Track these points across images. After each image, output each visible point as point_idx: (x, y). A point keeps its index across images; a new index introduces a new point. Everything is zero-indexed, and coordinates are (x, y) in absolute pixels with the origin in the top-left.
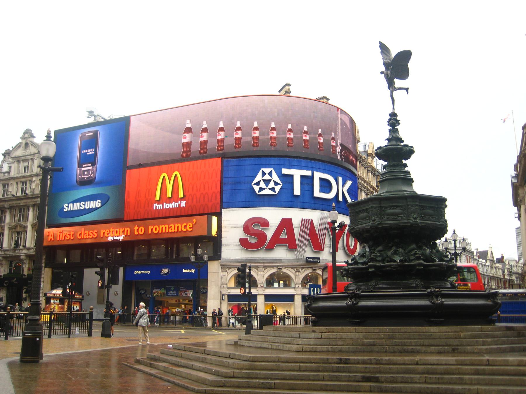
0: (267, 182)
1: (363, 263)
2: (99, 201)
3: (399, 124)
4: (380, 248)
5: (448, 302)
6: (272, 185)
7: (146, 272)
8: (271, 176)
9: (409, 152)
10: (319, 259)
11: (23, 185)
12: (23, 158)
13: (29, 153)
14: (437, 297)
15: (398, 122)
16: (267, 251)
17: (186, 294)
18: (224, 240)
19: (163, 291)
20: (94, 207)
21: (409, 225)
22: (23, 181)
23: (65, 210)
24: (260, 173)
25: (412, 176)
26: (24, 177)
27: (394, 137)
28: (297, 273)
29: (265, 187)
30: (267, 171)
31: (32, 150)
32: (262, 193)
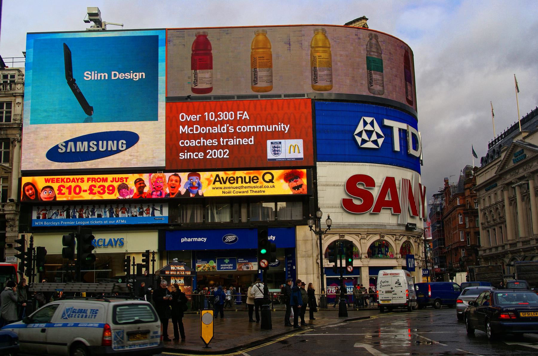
0: (369, 133)
2: (124, 142)
6: (374, 137)
7: (200, 240)
8: (373, 126)
10: (415, 225)
16: (371, 214)
17: (248, 268)
18: (321, 202)
19: (212, 264)
20: (115, 149)
23: (60, 151)
24: (362, 122)
28: (397, 242)
29: (368, 140)
30: (369, 120)
32: (365, 146)
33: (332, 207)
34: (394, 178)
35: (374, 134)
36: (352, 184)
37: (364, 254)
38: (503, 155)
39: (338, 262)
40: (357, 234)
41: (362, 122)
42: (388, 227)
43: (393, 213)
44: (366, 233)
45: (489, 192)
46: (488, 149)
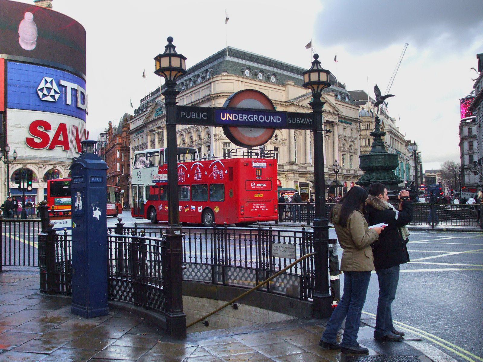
0: (49, 89)
6: (52, 93)
8: (52, 85)
16: (48, 150)
24: (43, 81)
29: (47, 94)
30: (49, 79)
32: (44, 99)
33: (18, 143)
34: (65, 124)
35: (53, 91)
36: (34, 127)
37: (41, 179)
38: (149, 109)
39: (22, 184)
40: (36, 164)
41: (44, 80)
42: (59, 160)
43: (63, 149)
44: (43, 164)
45: (139, 135)
46: (140, 104)
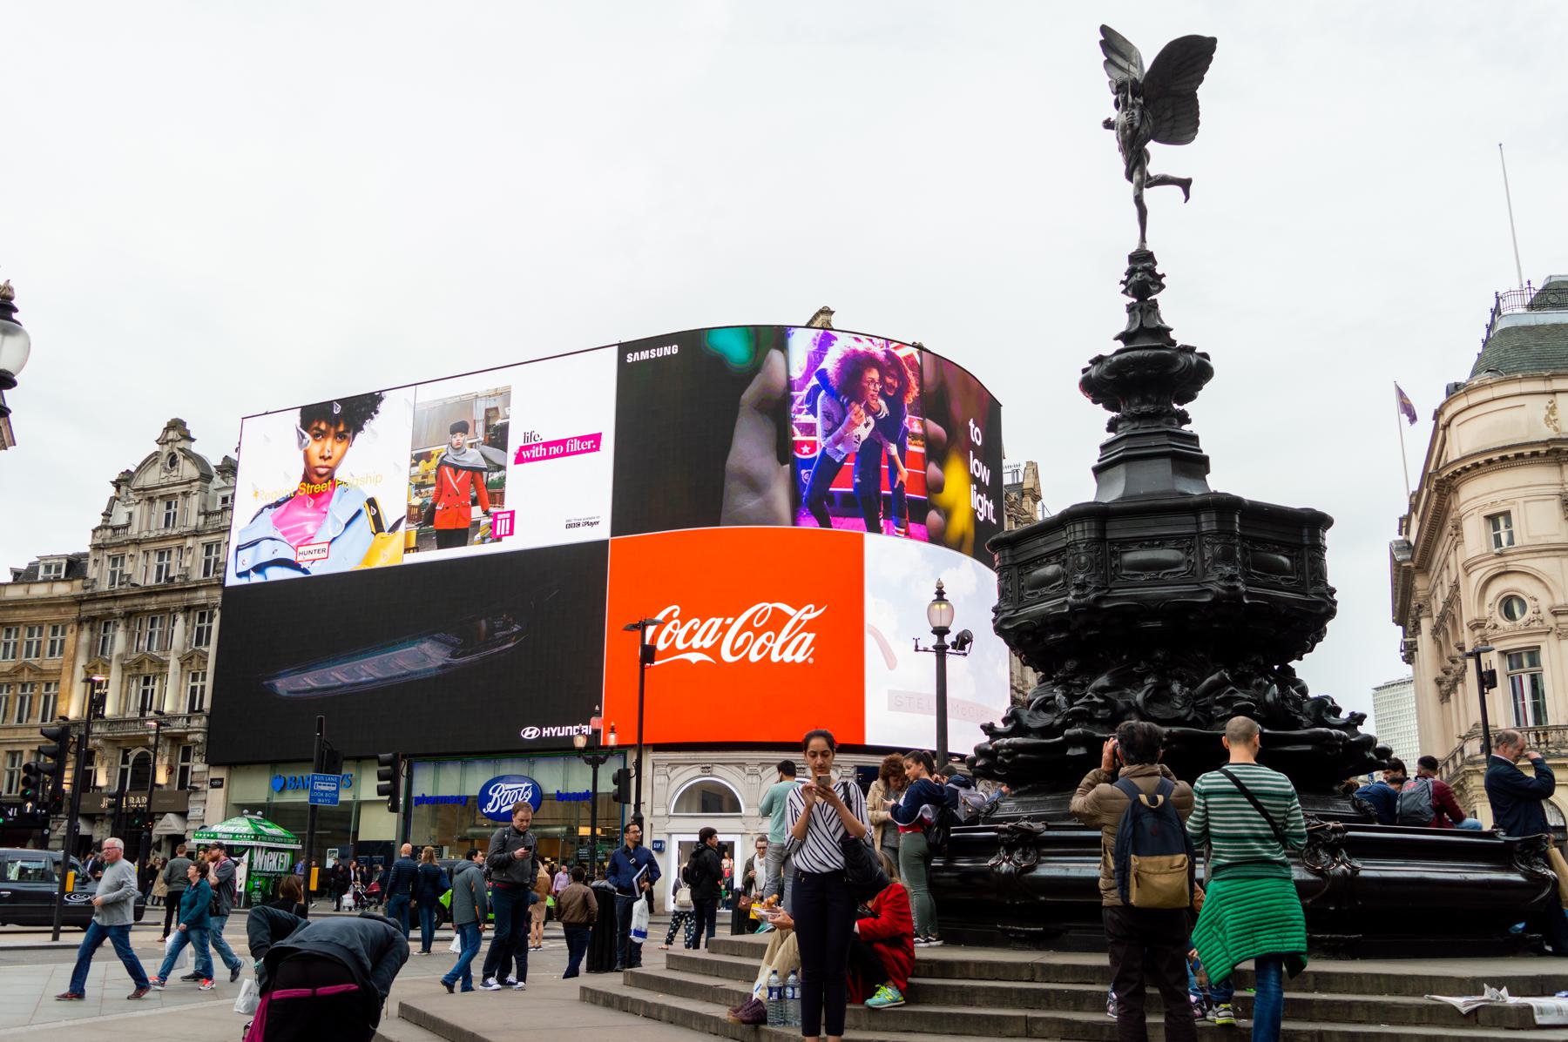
1: (1047, 731)
3: (1162, 287)
4: (1103, 681)
5: (1371, 870)
9: (1192, 373)
11: (161, 559)
12: (163, 491)
13: (177, 480)
14: (1333, 851)
15: (1157, 282)
21: (1208, 598)
22: (161, 546)
25: (1206, 447)
26: (164, 539)
27: (1146, 327)
31: (188, 470)
